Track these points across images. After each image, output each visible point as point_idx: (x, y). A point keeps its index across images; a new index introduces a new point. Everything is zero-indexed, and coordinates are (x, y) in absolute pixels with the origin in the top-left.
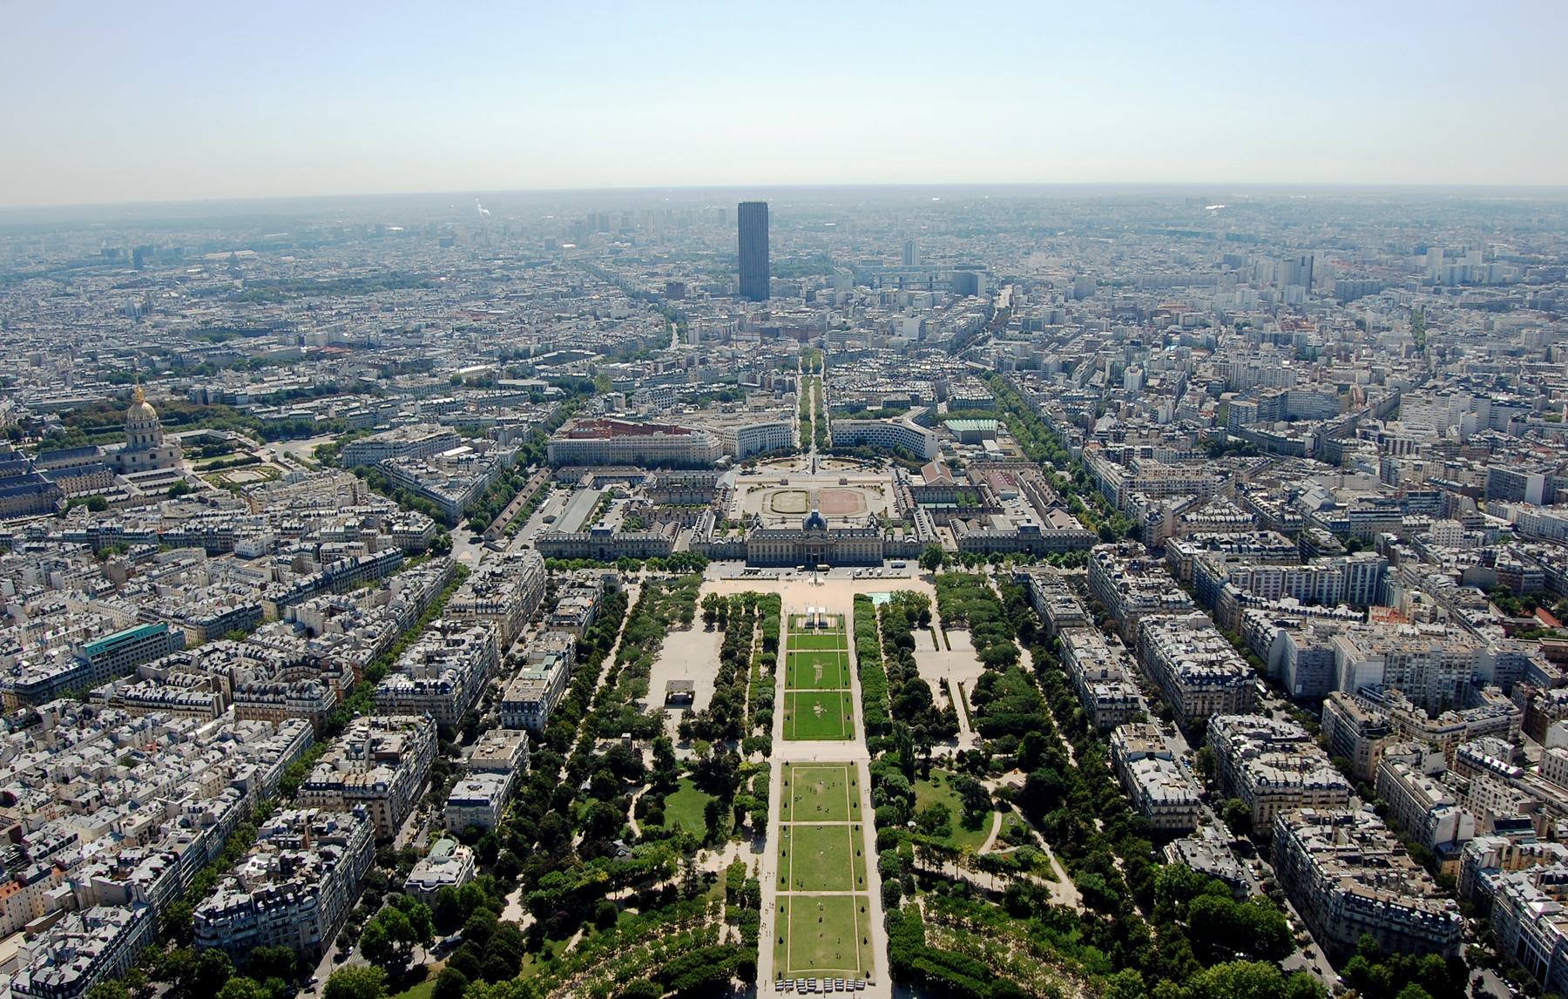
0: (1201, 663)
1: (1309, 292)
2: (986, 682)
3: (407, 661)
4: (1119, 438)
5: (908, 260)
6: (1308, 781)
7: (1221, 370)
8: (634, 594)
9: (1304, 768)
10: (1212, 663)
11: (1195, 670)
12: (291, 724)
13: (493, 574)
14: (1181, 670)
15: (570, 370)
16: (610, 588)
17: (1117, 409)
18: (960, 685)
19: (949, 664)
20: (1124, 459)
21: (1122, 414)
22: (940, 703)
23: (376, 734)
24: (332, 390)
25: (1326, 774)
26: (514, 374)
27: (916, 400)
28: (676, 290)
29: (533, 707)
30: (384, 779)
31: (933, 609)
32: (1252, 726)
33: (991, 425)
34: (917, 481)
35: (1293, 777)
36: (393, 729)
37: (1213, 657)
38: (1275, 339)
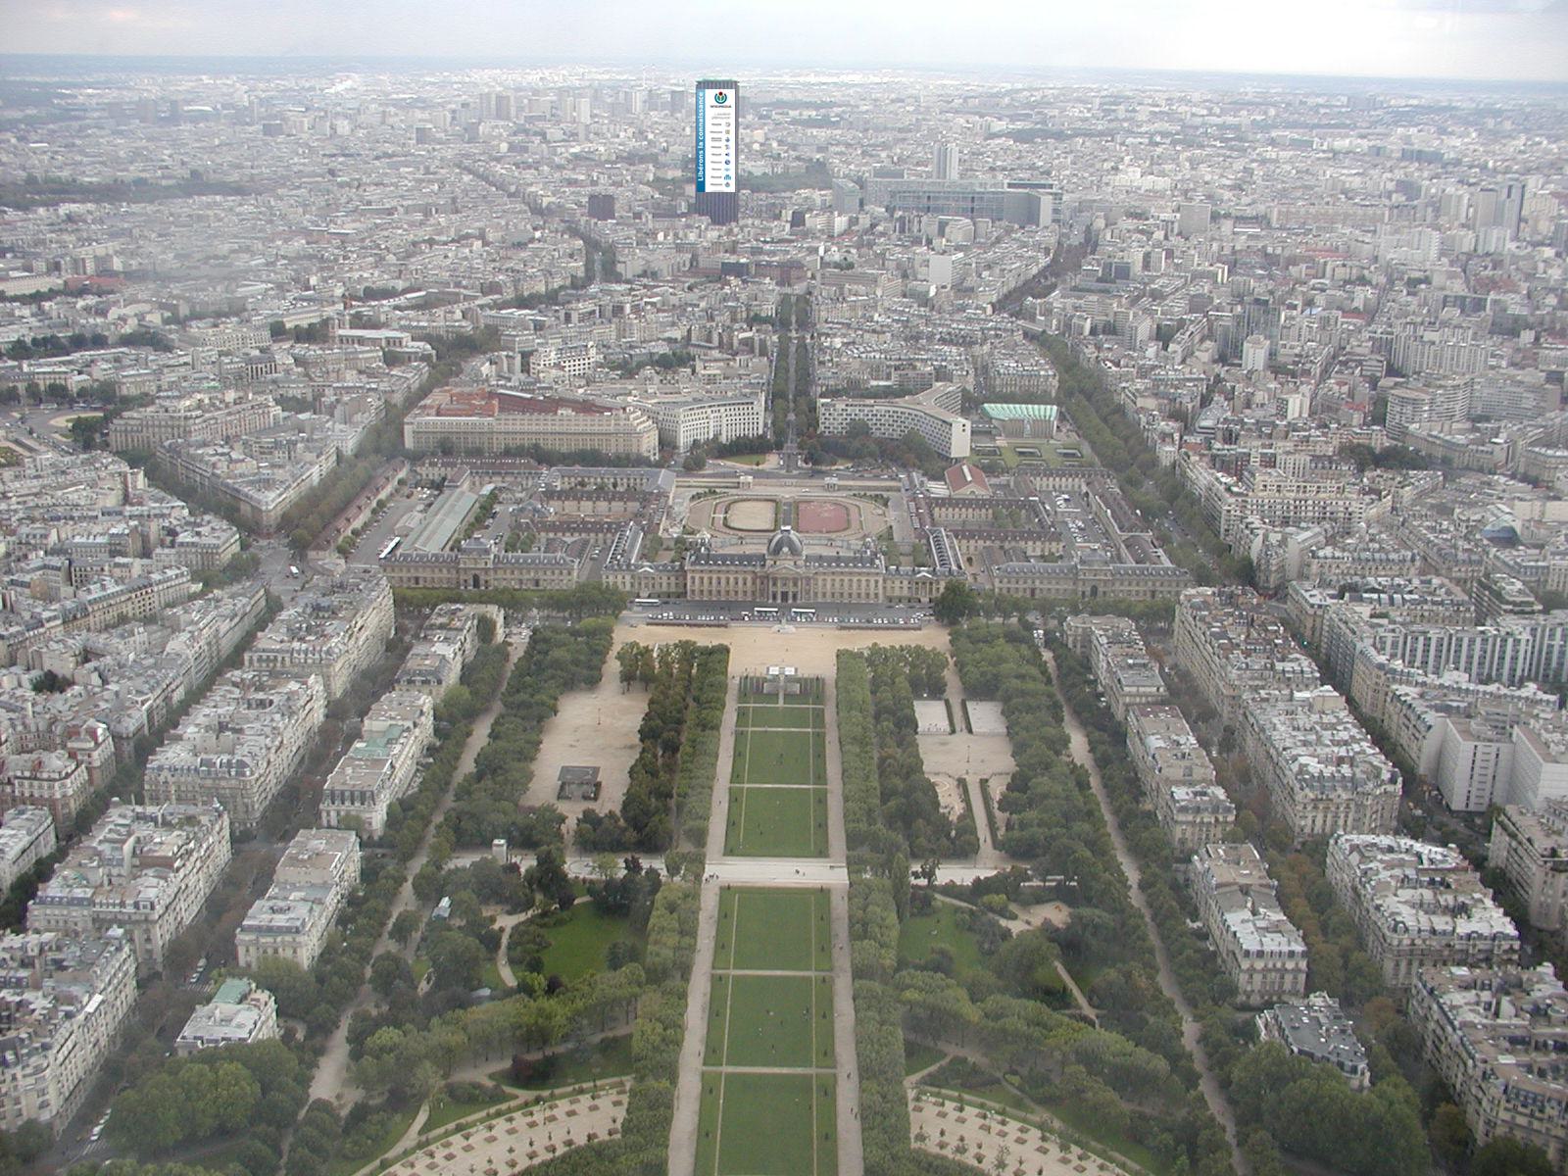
0: (1326, 761)
1: (1516, 238)
2: (1019, 783)
3: (189, 730)
4: (1230, 438)
5: (942, 170)
6: (1463, 927)
7: (1383, 346)
8: (521, 637)
9: (1462, 910)
10: (1340, 761)
11: (1314, 766)
12: (22, 812)
13: (317, 608)
14: (1295, 767)
15: (441, 320)
16: (485, 628)
17: (1230, 396)
18: (984, 783)
19: (963, 752)
20: (1237, 467)
21: (1239, 403)
22: (950, 801)
23: (143, 830)
24: (99, 341)
25: (1491, 920)
26: (358, 321)
27: (941, 374)
28: (602, 206)
29: (366, 797)
30: (151, 893)
31: (949, 675)
32: (1390, 850)
33: (1052, 411)
34: (938, 489)
35: (1441, 923)
36: (167, 825)
37: (1342, 752)
38: (1460, 302)
